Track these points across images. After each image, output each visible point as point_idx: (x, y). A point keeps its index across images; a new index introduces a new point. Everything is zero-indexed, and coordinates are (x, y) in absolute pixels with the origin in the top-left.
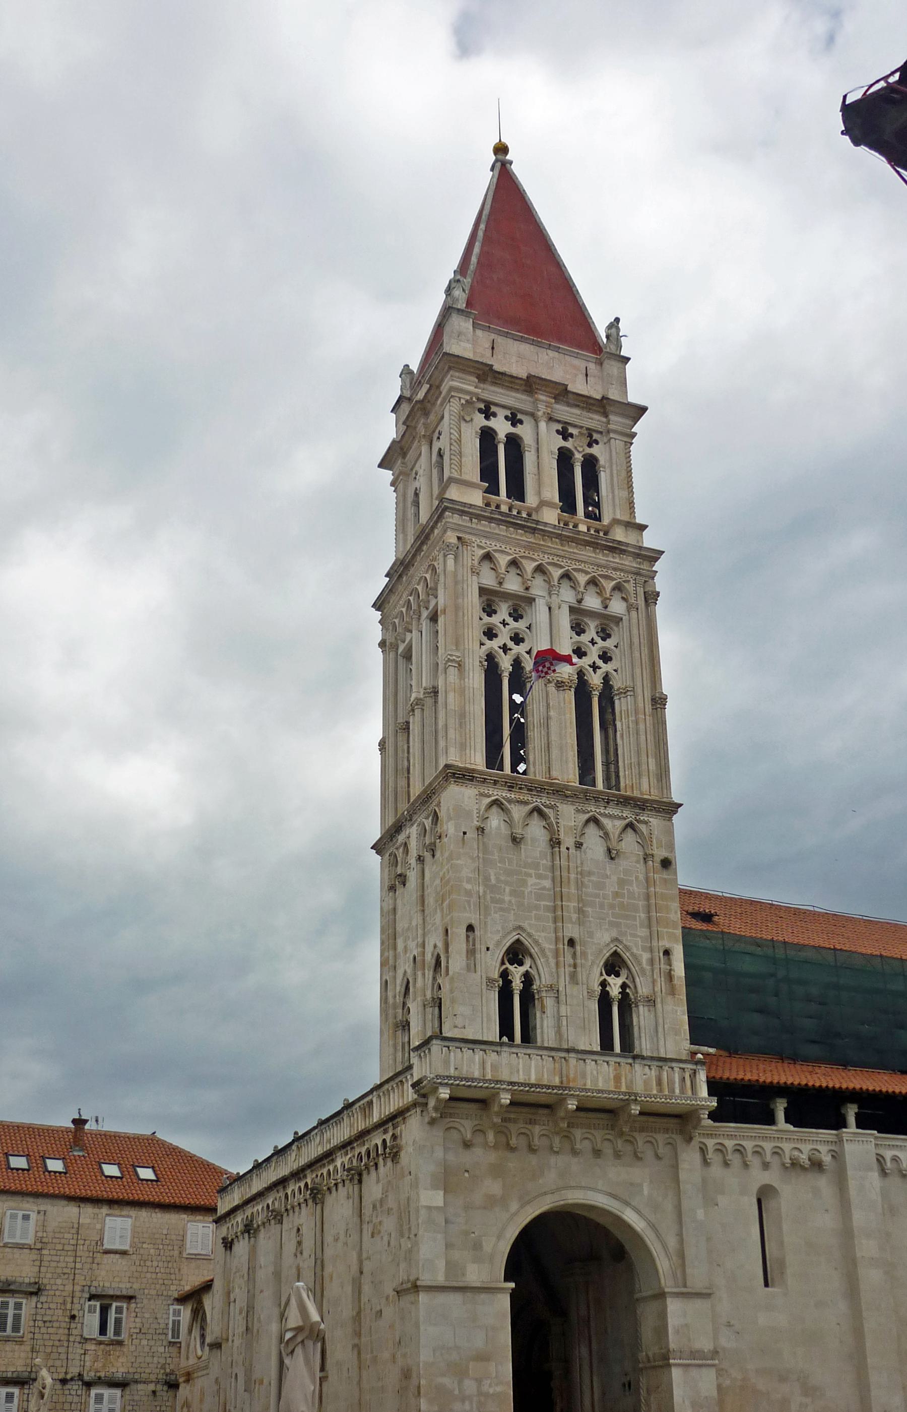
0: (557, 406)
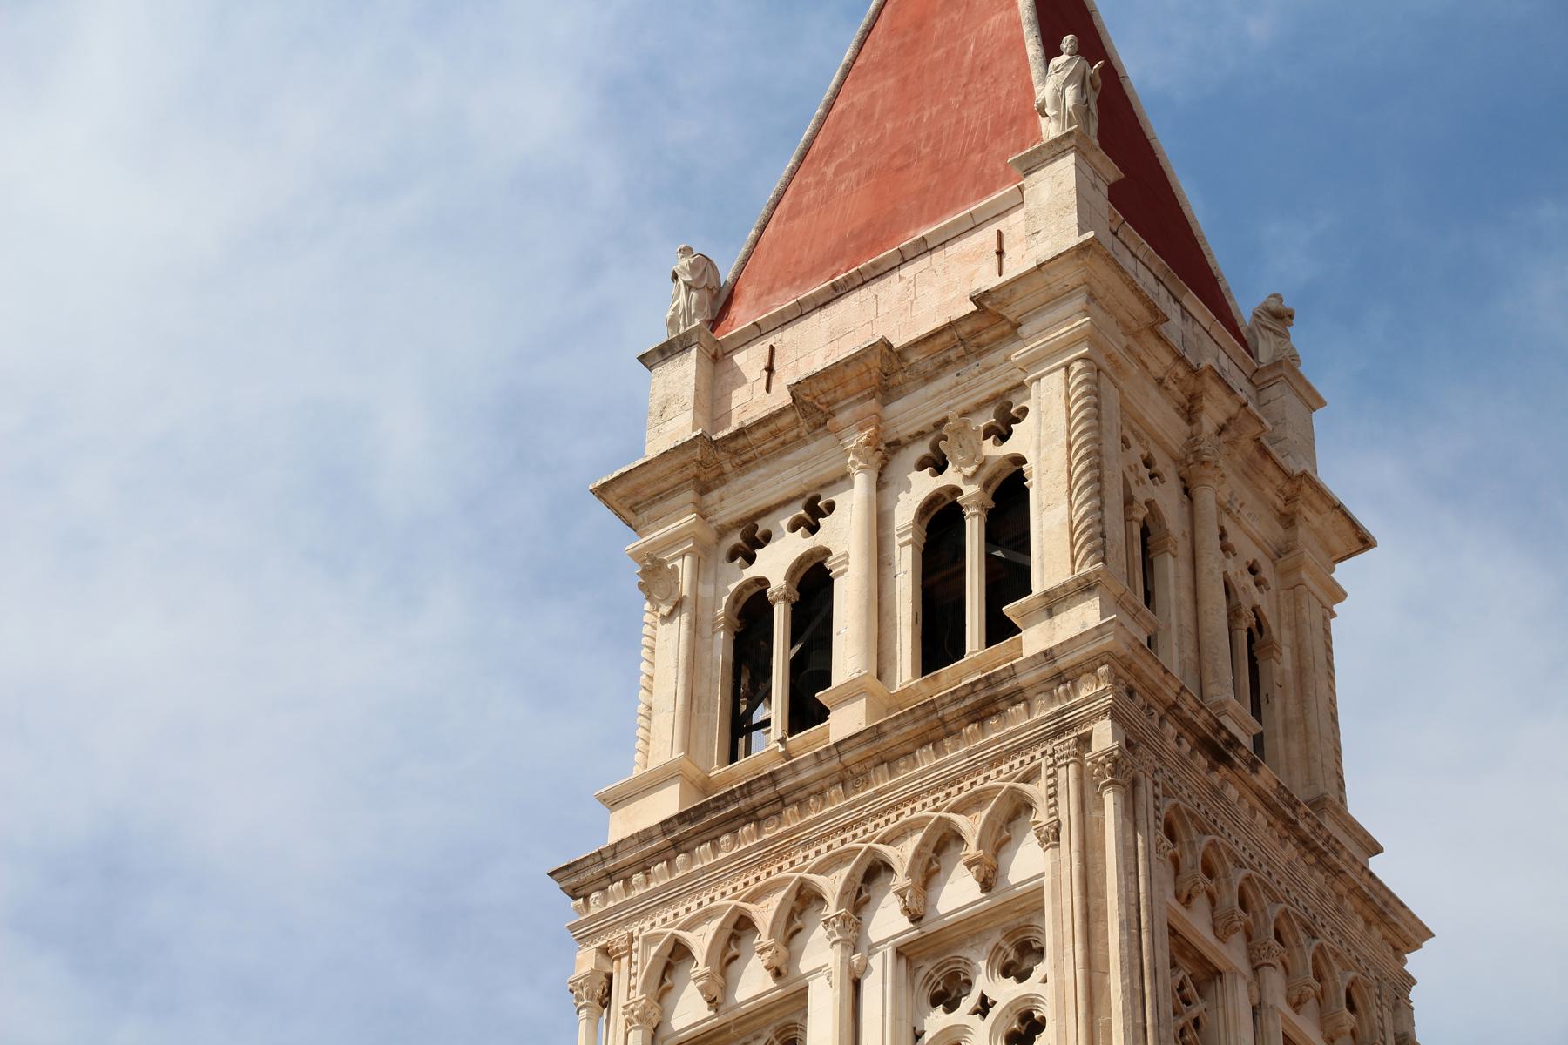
0: (896, 406)
